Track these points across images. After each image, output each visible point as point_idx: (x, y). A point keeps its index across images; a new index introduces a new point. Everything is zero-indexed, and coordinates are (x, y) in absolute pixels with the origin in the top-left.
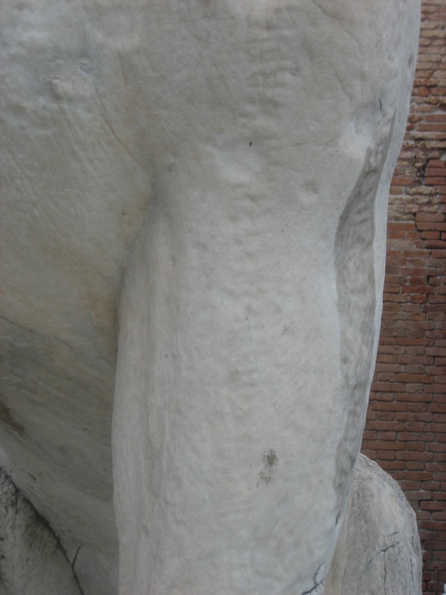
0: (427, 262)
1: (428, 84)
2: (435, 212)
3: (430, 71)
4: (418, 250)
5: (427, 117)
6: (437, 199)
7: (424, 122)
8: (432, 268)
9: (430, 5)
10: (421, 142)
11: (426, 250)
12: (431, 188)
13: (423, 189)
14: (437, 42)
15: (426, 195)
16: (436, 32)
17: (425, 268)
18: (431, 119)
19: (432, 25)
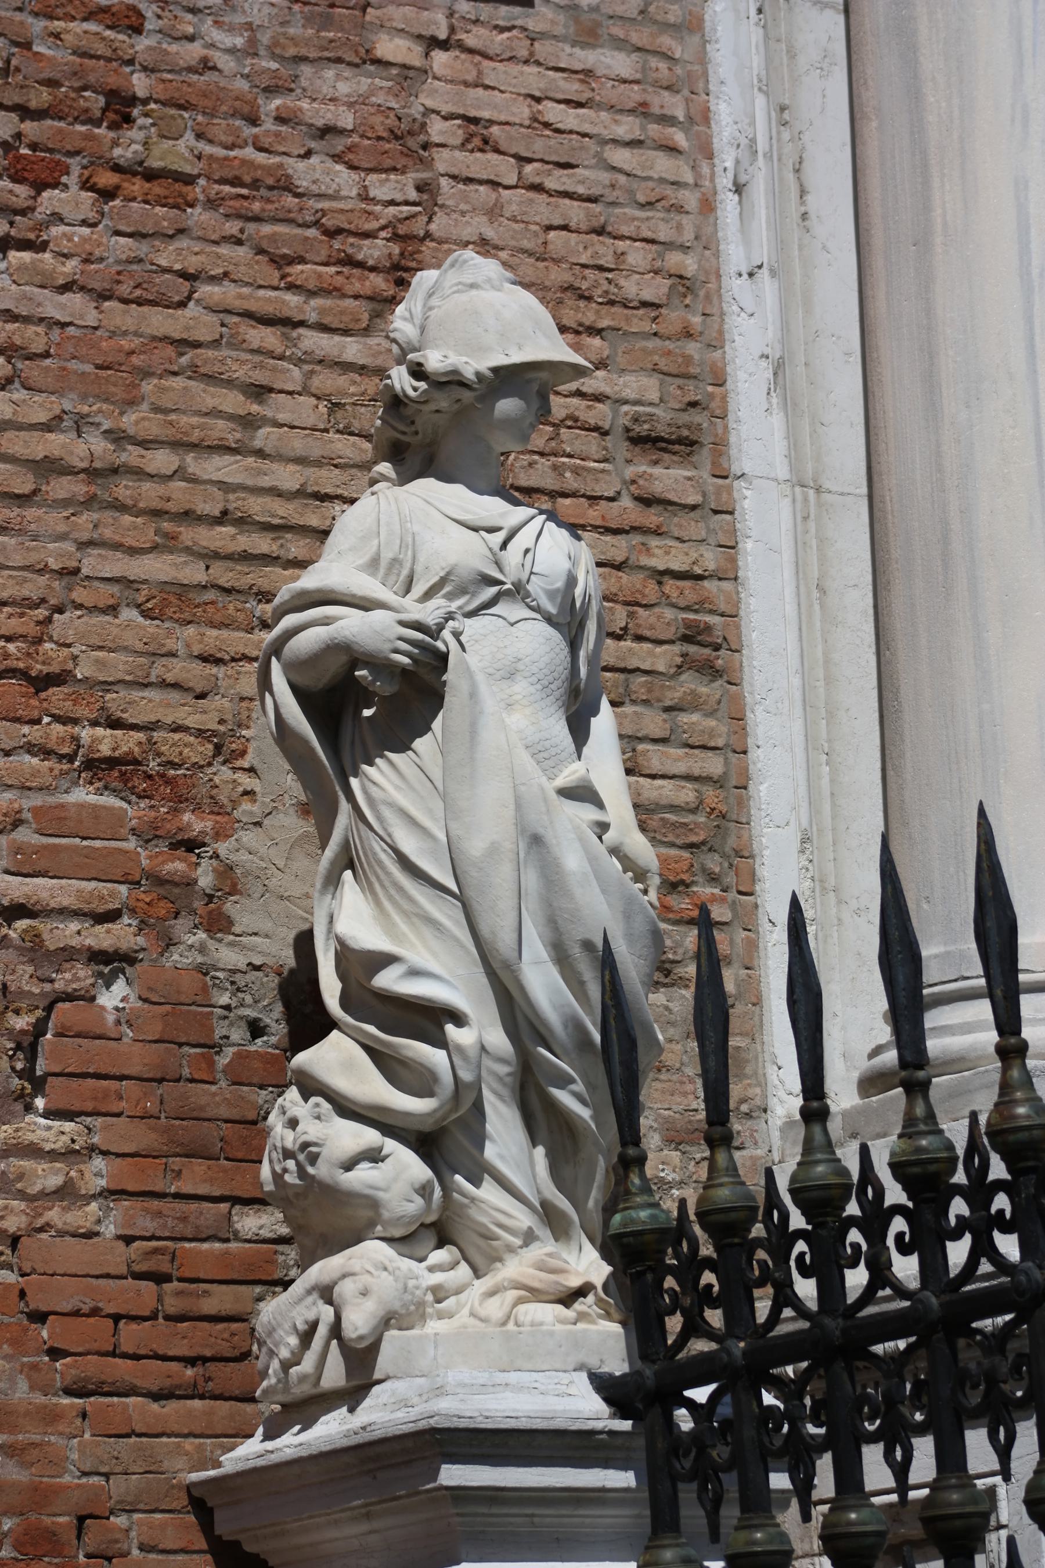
0: (75, 1456)
1: (37, 668)
2: (90, 1235)
3: (42, 613)
4: (39, 1399)
5: (36, 811)
6: (97, 1174)
7: (24, 835)
8: (95, 1479)
9: (27, 320)
10: (22, 924)
11: (66, 1401)
12: (68, 1126)
13: (41, 1129)
14: (61, 487)
15: (53, 1155)
16: (55, 443)
17: (67, 1479)
18: (54, 821)
19: (39, 409)
